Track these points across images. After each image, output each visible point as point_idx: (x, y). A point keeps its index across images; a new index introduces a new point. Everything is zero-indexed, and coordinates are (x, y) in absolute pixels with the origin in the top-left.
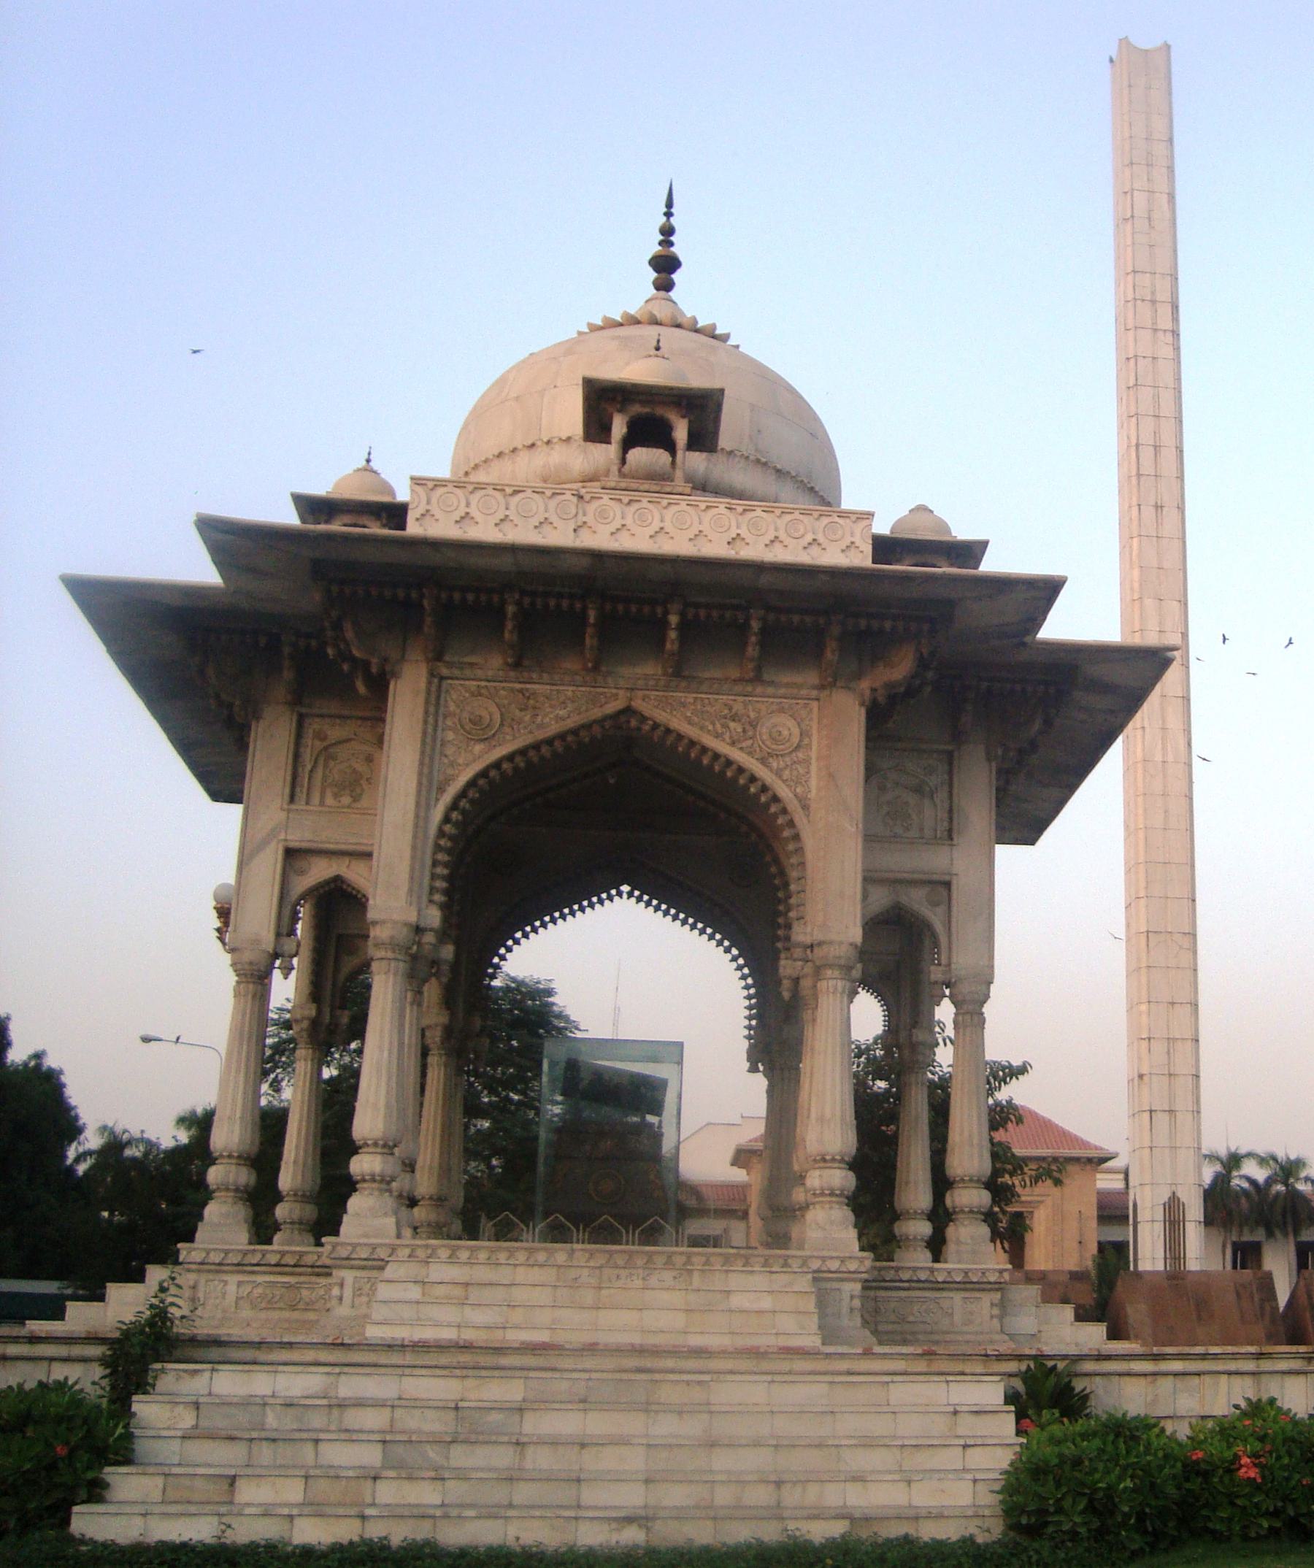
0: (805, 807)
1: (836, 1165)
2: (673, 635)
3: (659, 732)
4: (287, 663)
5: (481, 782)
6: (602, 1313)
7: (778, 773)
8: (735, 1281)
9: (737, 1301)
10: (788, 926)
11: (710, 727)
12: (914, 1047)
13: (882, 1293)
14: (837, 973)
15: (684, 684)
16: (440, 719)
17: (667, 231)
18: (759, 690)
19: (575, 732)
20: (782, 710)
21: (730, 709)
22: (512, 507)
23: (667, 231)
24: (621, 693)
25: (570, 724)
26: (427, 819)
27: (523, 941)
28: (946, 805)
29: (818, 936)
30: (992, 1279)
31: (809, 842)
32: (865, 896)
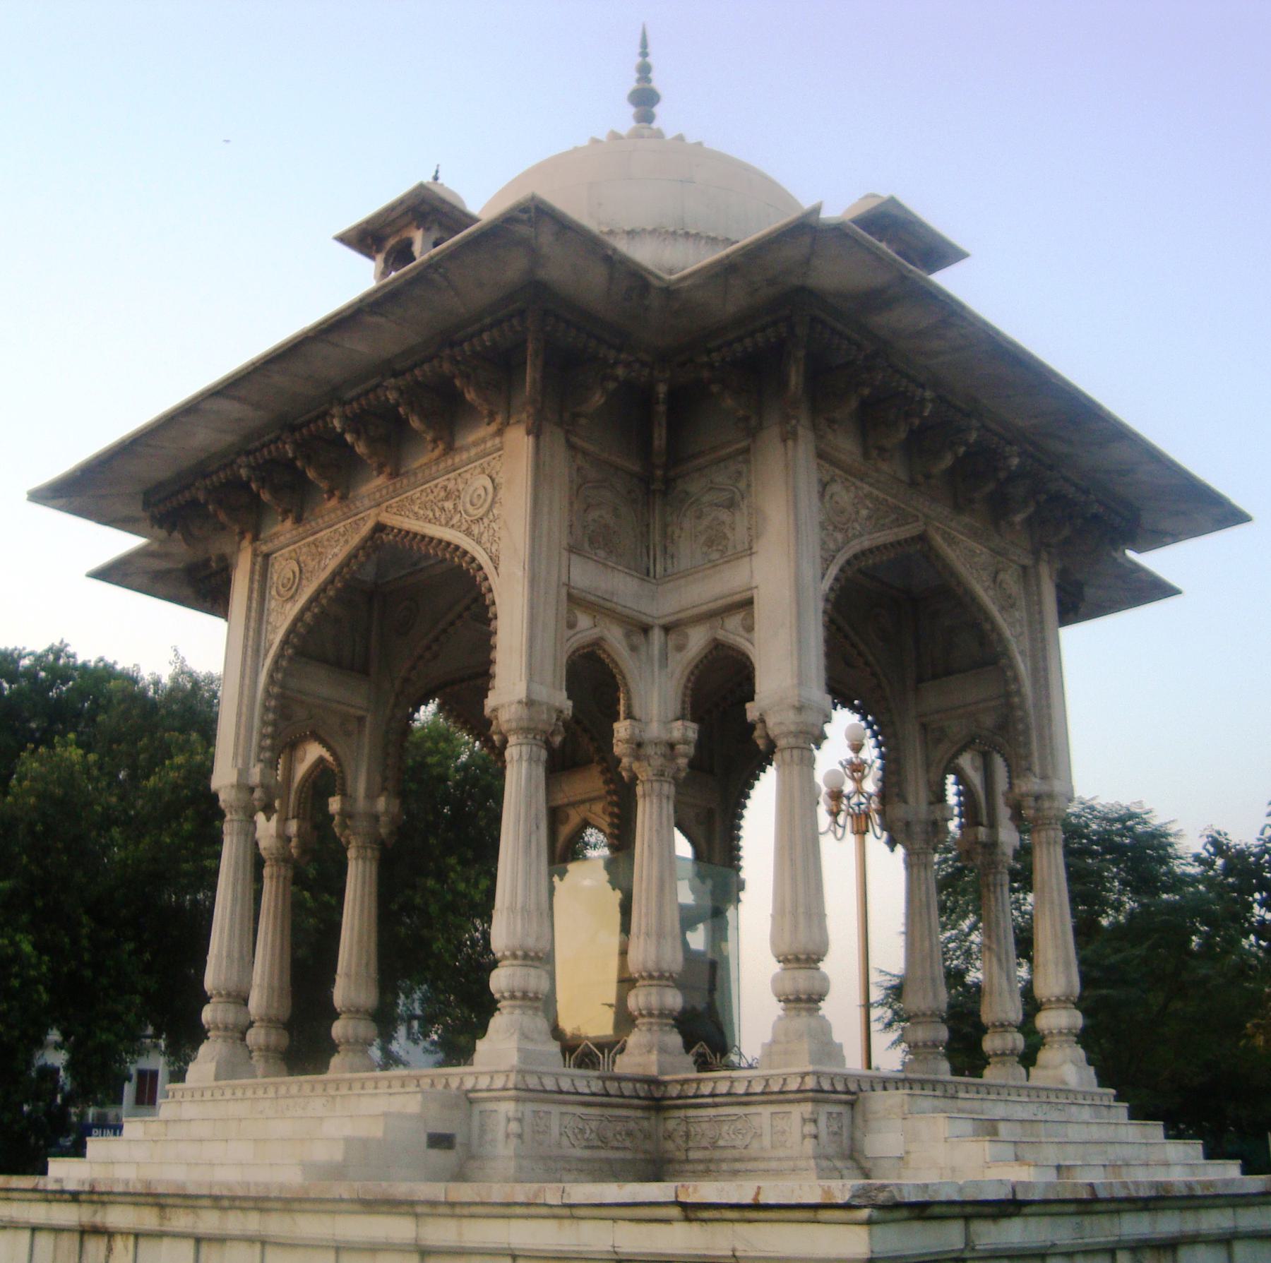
13: (691, 1112)
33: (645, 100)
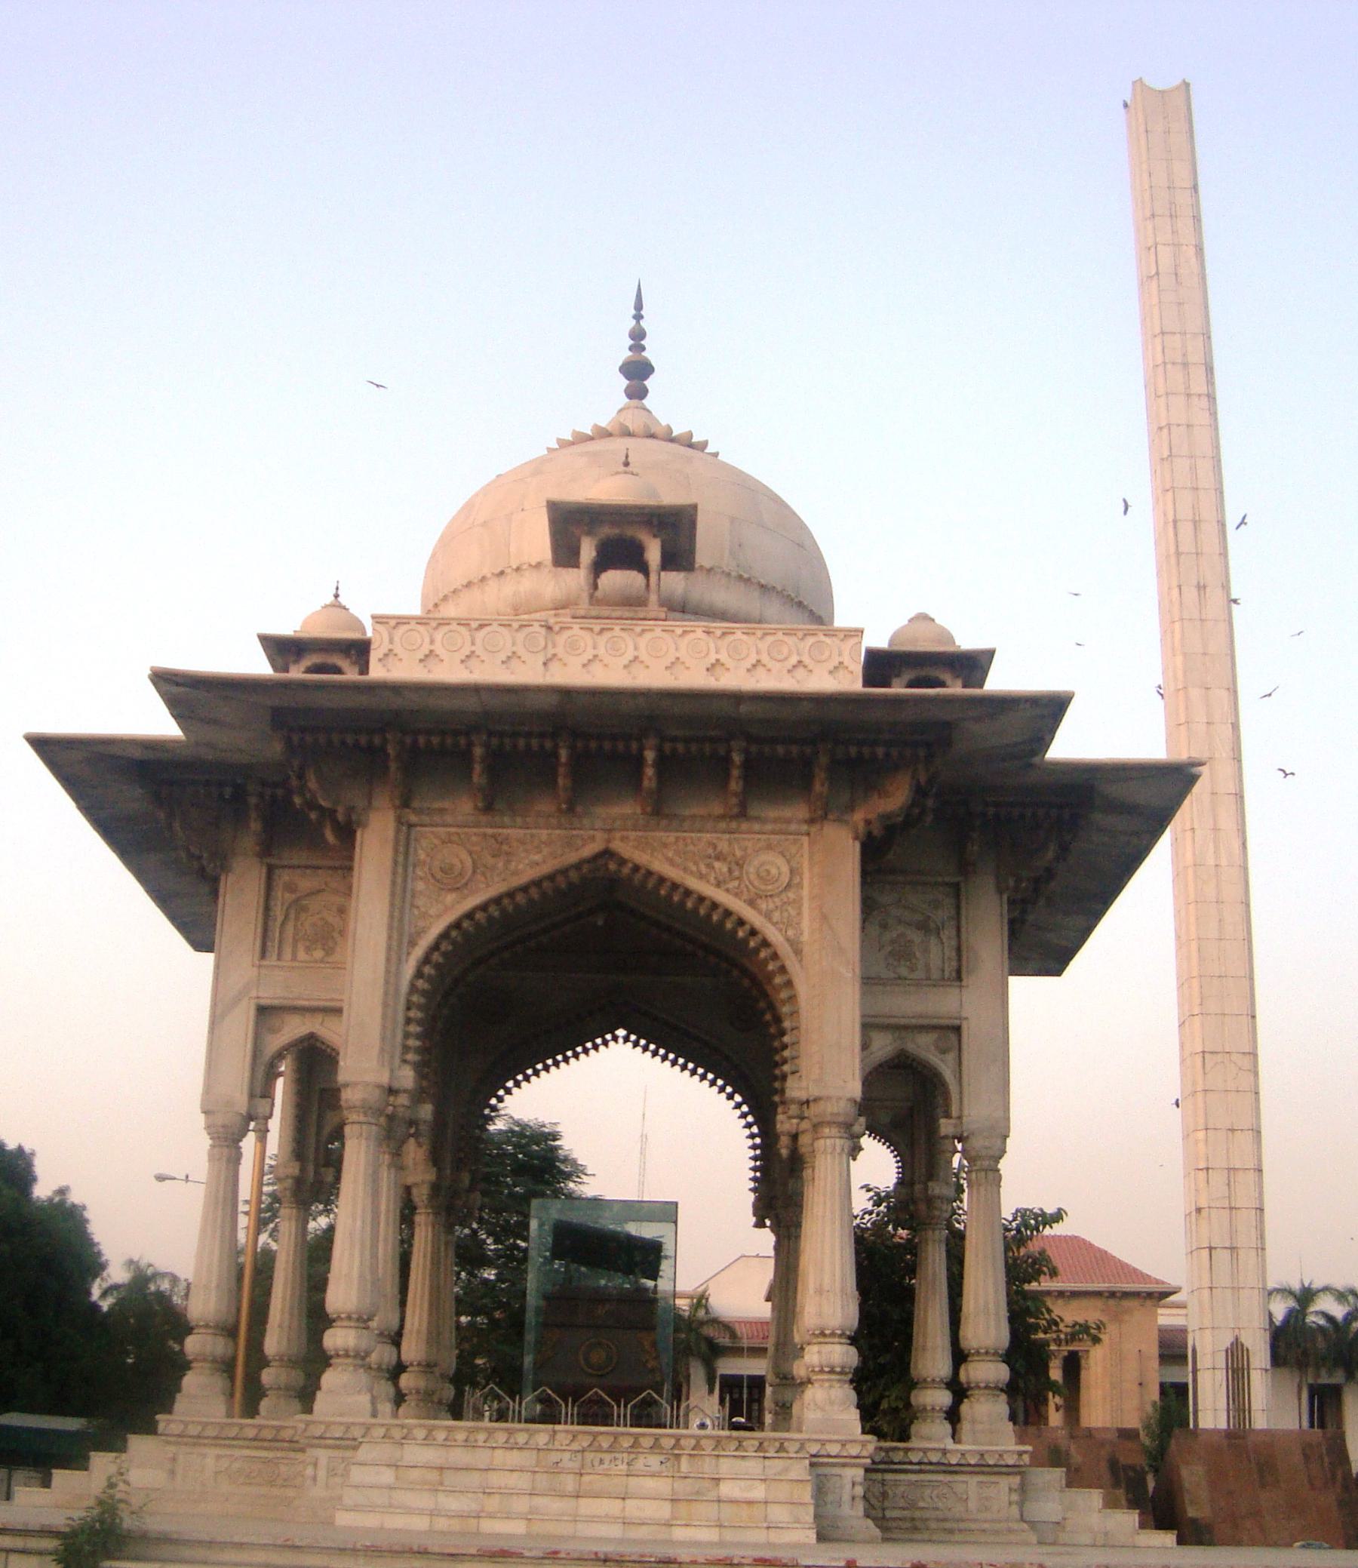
0: (798, 952)
1: (837, 1340)
2: (650, 772)
3: (638, 877)
5: (454, 934)
6: (582, 1501)
7: (768, 916)
8: (726, 1466)
9: (726, 1489)
10: (784, 1077)
11: (694, 868)
12: (930, 1201)
14: (834, 1131)
15: (664, 822)
16: (411, 869)
17: (638, 336)
18: (745, 826)
19: (551, 877)
20: (769, 847)
21: (715, 847)
22: (478, 641)
23: (638, 336)
24: (599, 835)
25: (546, 869)
26: (398, 974)
27: (515, 1090)
28: (954, 943)
29: (814, 1091)
30: (1011, 1462)
31: (802, 989)
32: (865, 1046)
33: (637, 372)
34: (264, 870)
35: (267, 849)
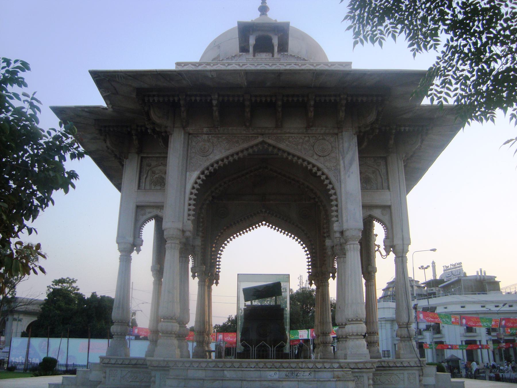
4: (134, 137)
34: (140, 158)
35: (140, 151)
